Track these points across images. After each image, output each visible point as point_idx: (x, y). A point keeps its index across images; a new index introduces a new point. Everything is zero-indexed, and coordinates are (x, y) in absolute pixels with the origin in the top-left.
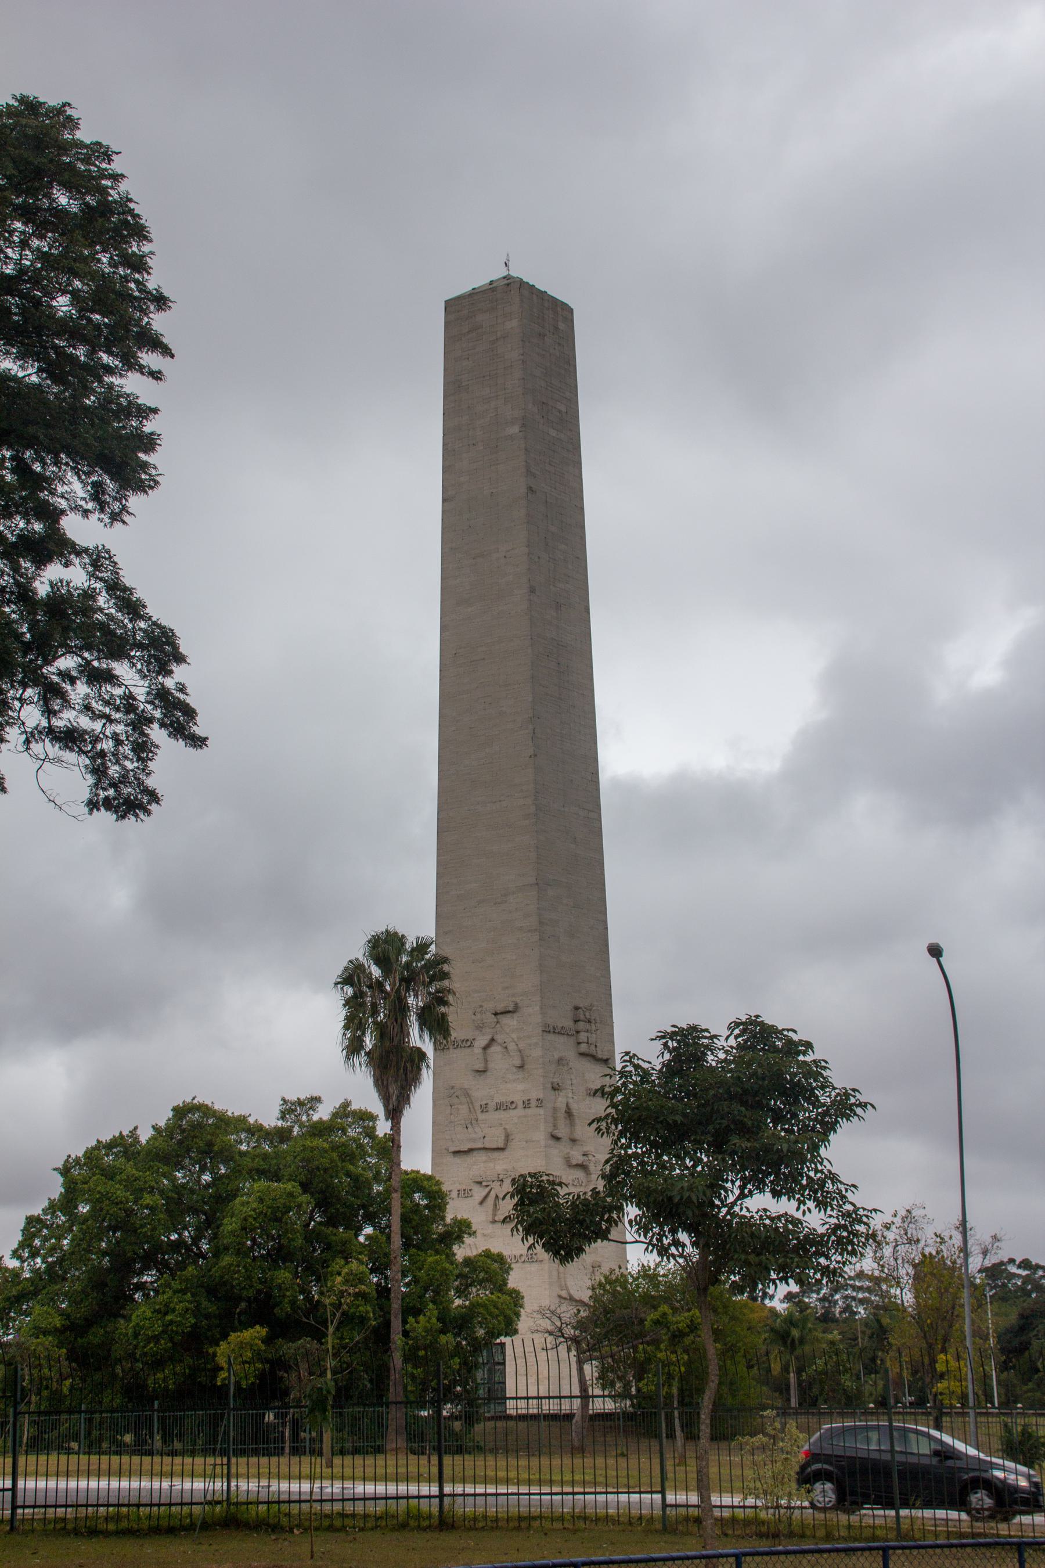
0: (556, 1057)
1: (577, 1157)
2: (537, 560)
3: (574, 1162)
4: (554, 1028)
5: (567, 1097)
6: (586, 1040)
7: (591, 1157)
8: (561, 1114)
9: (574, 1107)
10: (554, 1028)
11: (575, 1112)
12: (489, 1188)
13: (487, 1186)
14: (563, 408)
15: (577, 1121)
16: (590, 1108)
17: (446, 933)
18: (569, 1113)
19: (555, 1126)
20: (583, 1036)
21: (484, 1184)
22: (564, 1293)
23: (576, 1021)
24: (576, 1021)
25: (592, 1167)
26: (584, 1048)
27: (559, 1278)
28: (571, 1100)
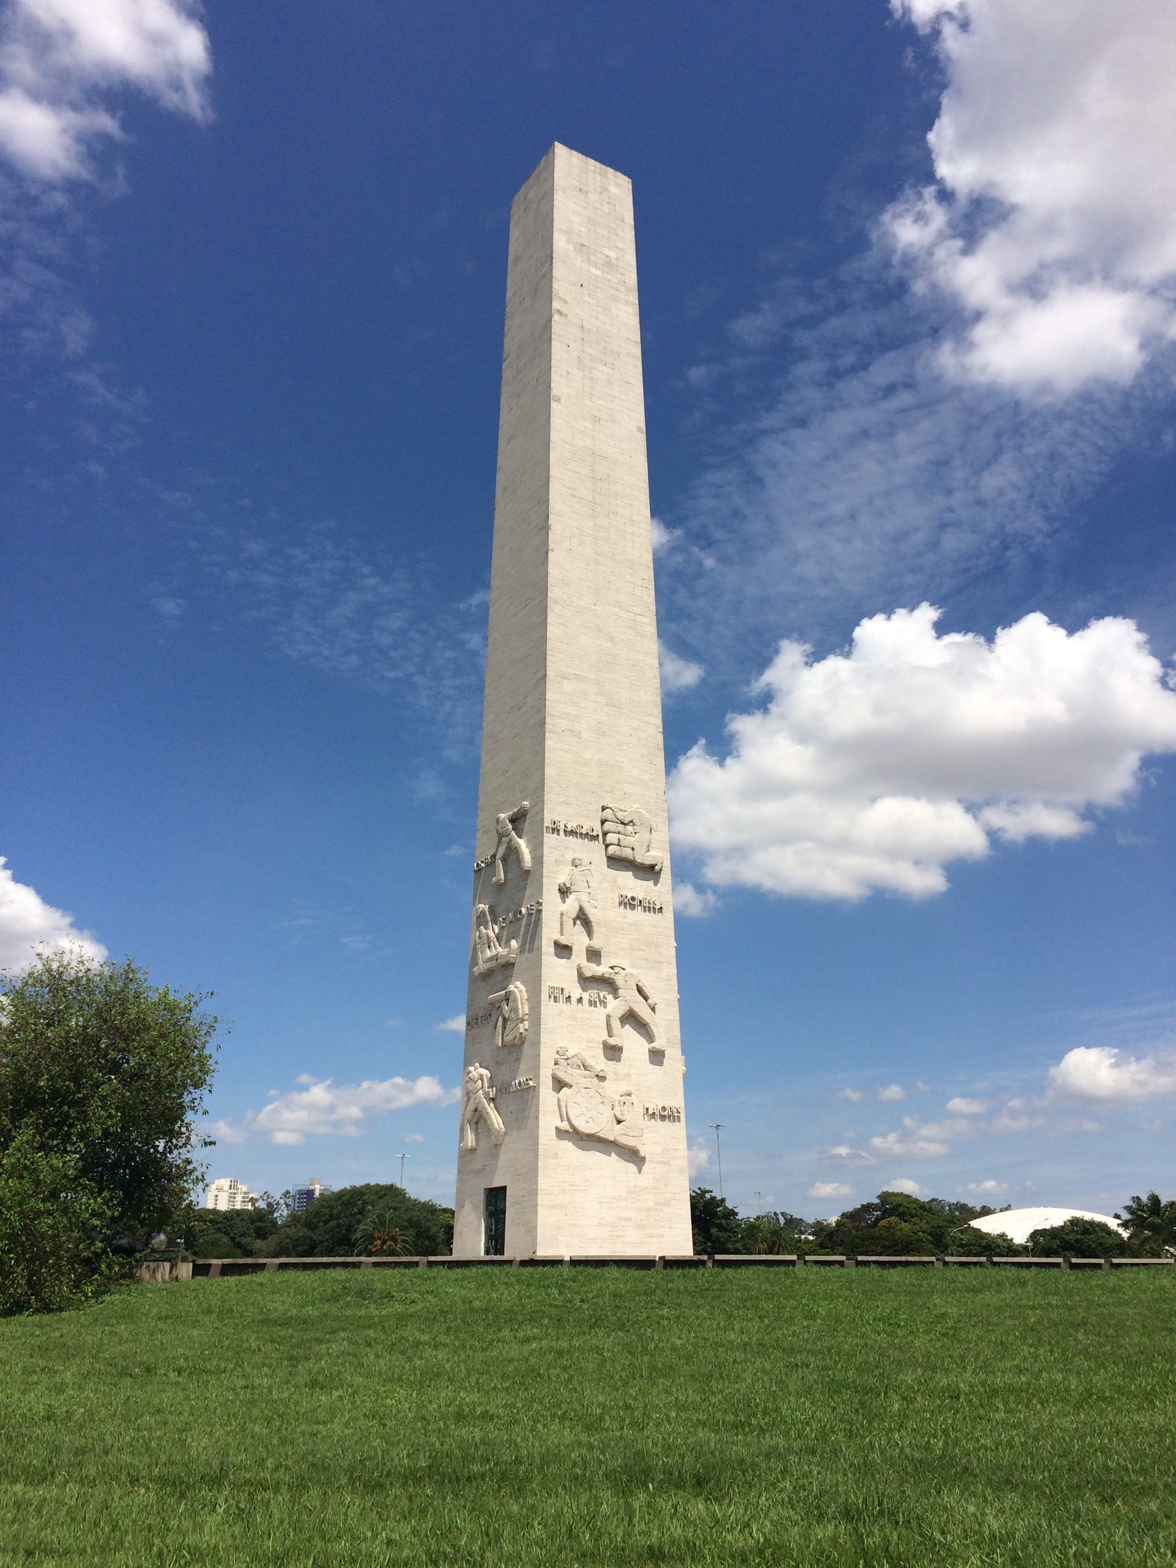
0: (569, 856)
2: (564, 373)
3: (588, 974)
4: (566, 826)
5: (579, 900)
6: (616, 842)
8: (568, 922)
9: (593, 914)
10: (566, 826)
11: (592, 918)
14: (613, 255)
15: (595, 928)
16: (625, 918)
18: (583, 919)
20: (611, 838)
22: (565, 1125)
23: (603, 822)
24: (603, 822)
25: (619, 981)
26: (612, 850)
27: (559, 1107)
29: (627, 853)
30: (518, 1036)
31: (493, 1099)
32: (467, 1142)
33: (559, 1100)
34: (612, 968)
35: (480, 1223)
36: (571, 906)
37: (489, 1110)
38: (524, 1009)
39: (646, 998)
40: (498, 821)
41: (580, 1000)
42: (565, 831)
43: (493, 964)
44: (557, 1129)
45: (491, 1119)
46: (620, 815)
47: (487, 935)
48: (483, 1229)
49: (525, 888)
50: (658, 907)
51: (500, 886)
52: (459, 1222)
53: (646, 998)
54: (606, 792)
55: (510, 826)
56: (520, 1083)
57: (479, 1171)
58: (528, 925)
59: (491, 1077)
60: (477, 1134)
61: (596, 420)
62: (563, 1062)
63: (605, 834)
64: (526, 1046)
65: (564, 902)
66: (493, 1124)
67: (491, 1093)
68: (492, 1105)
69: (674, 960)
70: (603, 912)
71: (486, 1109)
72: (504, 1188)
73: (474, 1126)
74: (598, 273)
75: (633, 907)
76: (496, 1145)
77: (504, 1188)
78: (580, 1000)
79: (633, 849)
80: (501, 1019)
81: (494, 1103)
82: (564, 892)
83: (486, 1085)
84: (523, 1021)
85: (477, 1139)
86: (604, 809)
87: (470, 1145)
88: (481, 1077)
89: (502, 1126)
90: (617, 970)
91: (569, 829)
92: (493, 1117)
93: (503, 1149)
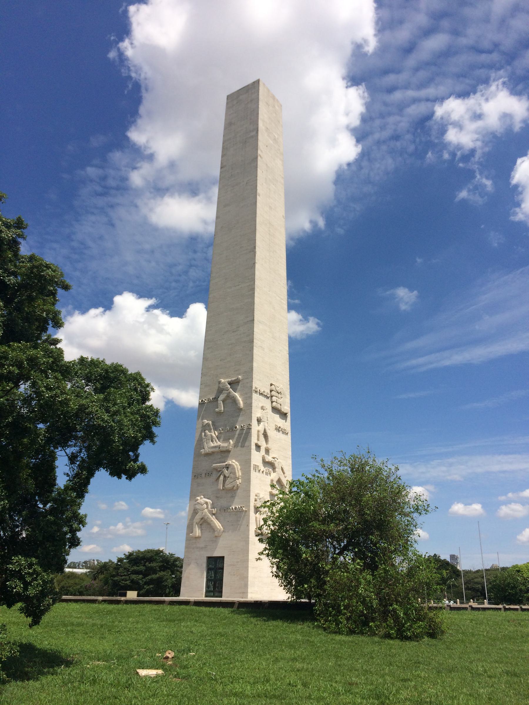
0: (261, 405)
1: (269, 458)
3: (267, 460)
4: (260, 391)
5: (265, 426)
7: (276, 459)
9: (269, 433)
10: (260, 391)
11: (269, 434)
12: (221, 472)
13: (220, 471)
17: (208, 348)
18: (265, 435)
19: (258, 440)
20: (274, 399)
21: (219, 470)
24: (271, 391)
25: (276, 465)
27: (256, 521)
28: (267, 428)
29: (279, 406)
30: (236, 486)
31: (214, 514)
32: (196, 533)
33: (256, 518)
34: (274, 458)
35: (203, 573)
36: (261, 427)
37: (212, 519)
38: (239, 473)
39: (284, 473)
40: (220, 382)
41: (263, 472)
42: (259, 393)
43: (217, 449)
44: (255, 531)
45: (215, 524)
46: (277, 389)
47: (211, 435)
48: (205, 576)
49: (238, 416)
50: (287, 432)
51: (220, 413)
52: (187, 571)
53: (284, 473)
54: (272, 377)
55: (229, 386)
56: (236, 508)
57: (202, 548)
58: (240, 434)
59: (212, 503)
60: (201, 530)
61: (270, 208)
62: (258, 500)
63: (272, 396)
64: (239, 491)
65: (259, 426)
66: (216, 526)
67: (214, 511)
68: (214, 517)
69: (291, 457)
70: (271, 433)
71: (211, 519)
72: (223, 558)
73: (200, 526)
74: (272, 142)
75: (279, 431)
76: (216, 536)
77: (223, 558)
78: (263, 472)
79: (281, 405)
80: (222, 477)
81: (215, 516)
82: (259, 421)
83: (210, 507)
84: (238, 479)
85: (202, 532)
86: (271, 385)
87: (197, 535)
88: (206, 503)
89: (222, 528)
90: (276, 459)
91: (261, 392)
92: (216, 523)
93: (221, 539)
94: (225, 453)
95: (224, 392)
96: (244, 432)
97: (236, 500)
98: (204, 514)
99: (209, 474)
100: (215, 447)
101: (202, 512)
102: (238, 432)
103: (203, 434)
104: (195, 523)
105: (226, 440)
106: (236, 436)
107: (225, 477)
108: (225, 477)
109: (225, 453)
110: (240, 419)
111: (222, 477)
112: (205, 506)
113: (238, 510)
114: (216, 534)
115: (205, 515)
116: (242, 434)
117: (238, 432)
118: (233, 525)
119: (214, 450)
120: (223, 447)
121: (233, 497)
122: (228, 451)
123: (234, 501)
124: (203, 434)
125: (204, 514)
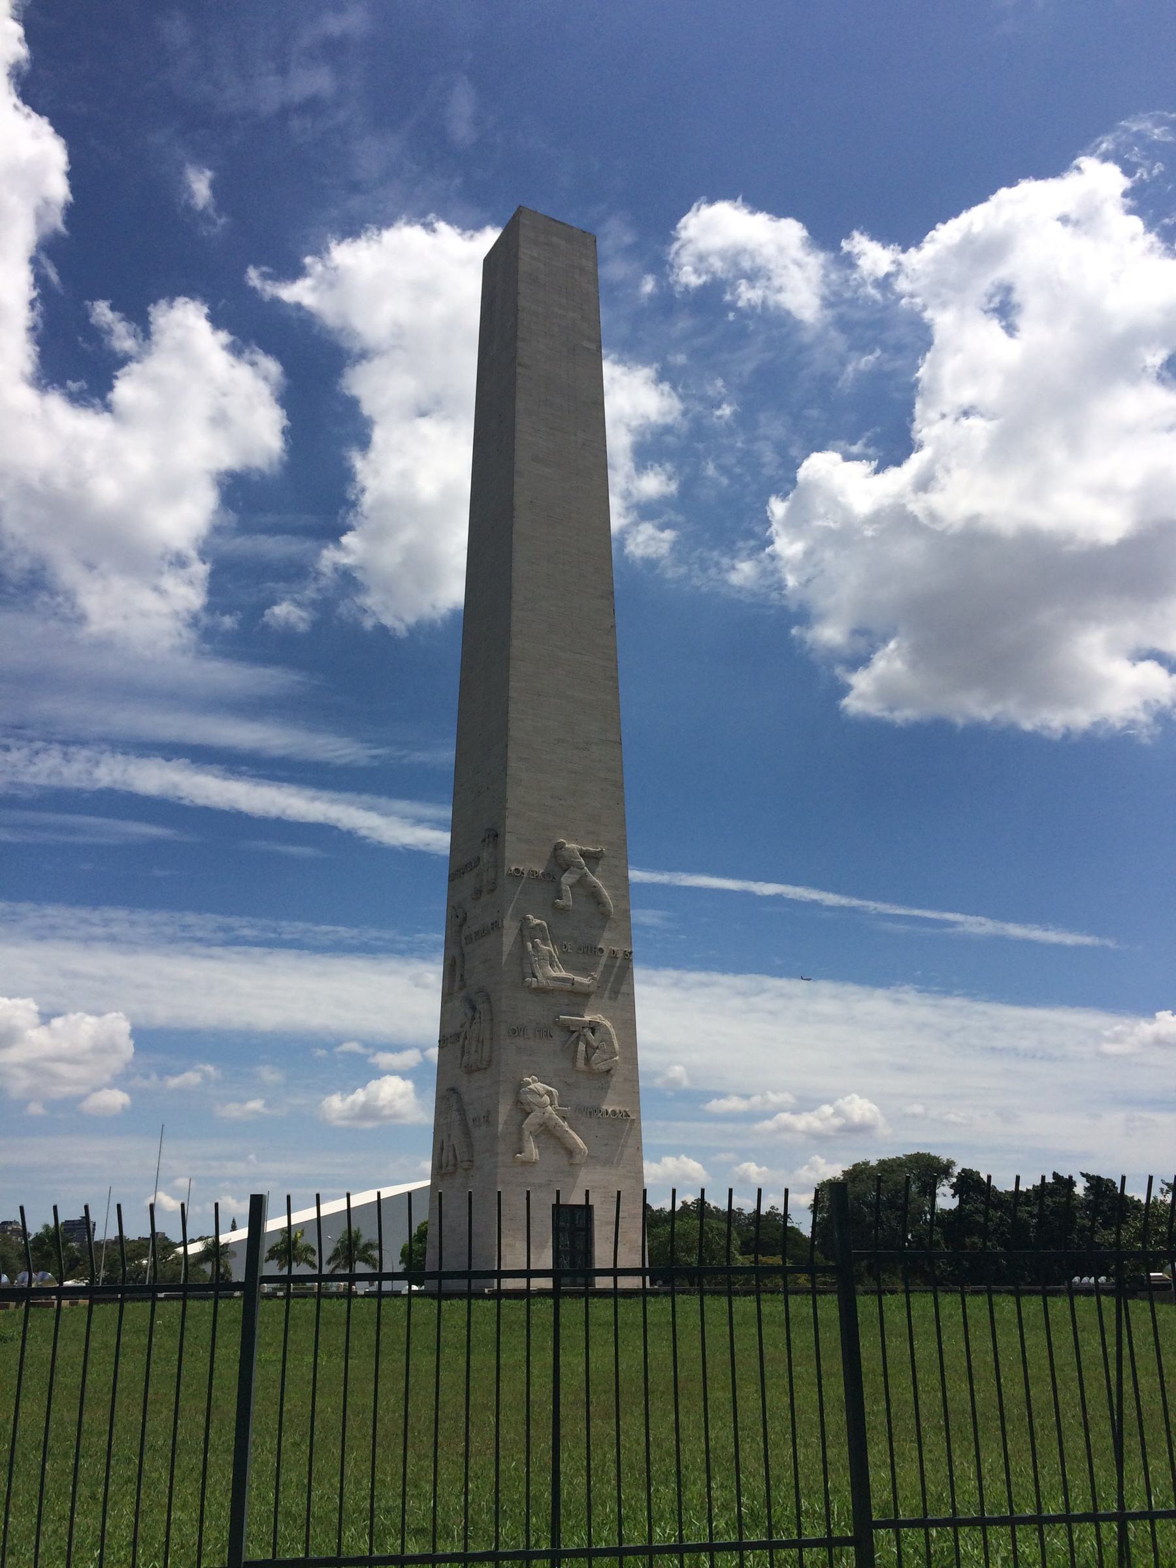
12: (576, 1034)
13: (573, 1032)
21: (572, 1029)
40: (559, 847)
43: (568, 986)
47: (550, 952)
51: (563, 910)
58: (608, 968)
80: (582, 1047)
88: (549, 1093)
94: (579, 997)
95: (572, 868)
96: (618, 965)
97: (611, 1095)
98: (547, 1115)
99: (545, 1033)
100: (563, 980)
101: (543, 1110)
102: (604, 960)
103: (530, 945)
104: (527, 1133)
105: (584, 971)
106: (601, 968)
107: (588, 1044)
108: (588, 1044)
109: (579, 997)
110: (607, 935)
111: (582, 1047)
112: (547, 1099)
113: (620, 1115)
114: (577, 1159)
115: (550, 1118)
116: (613, 966)
117: (604, 960)
118: (607, 1144)
119: (552, 984)
120: (581, 984)
121: (605, 1089)
122: (587, 995)
123: (605, 1096)
124: (530, 945)
125: (547, 1115)
